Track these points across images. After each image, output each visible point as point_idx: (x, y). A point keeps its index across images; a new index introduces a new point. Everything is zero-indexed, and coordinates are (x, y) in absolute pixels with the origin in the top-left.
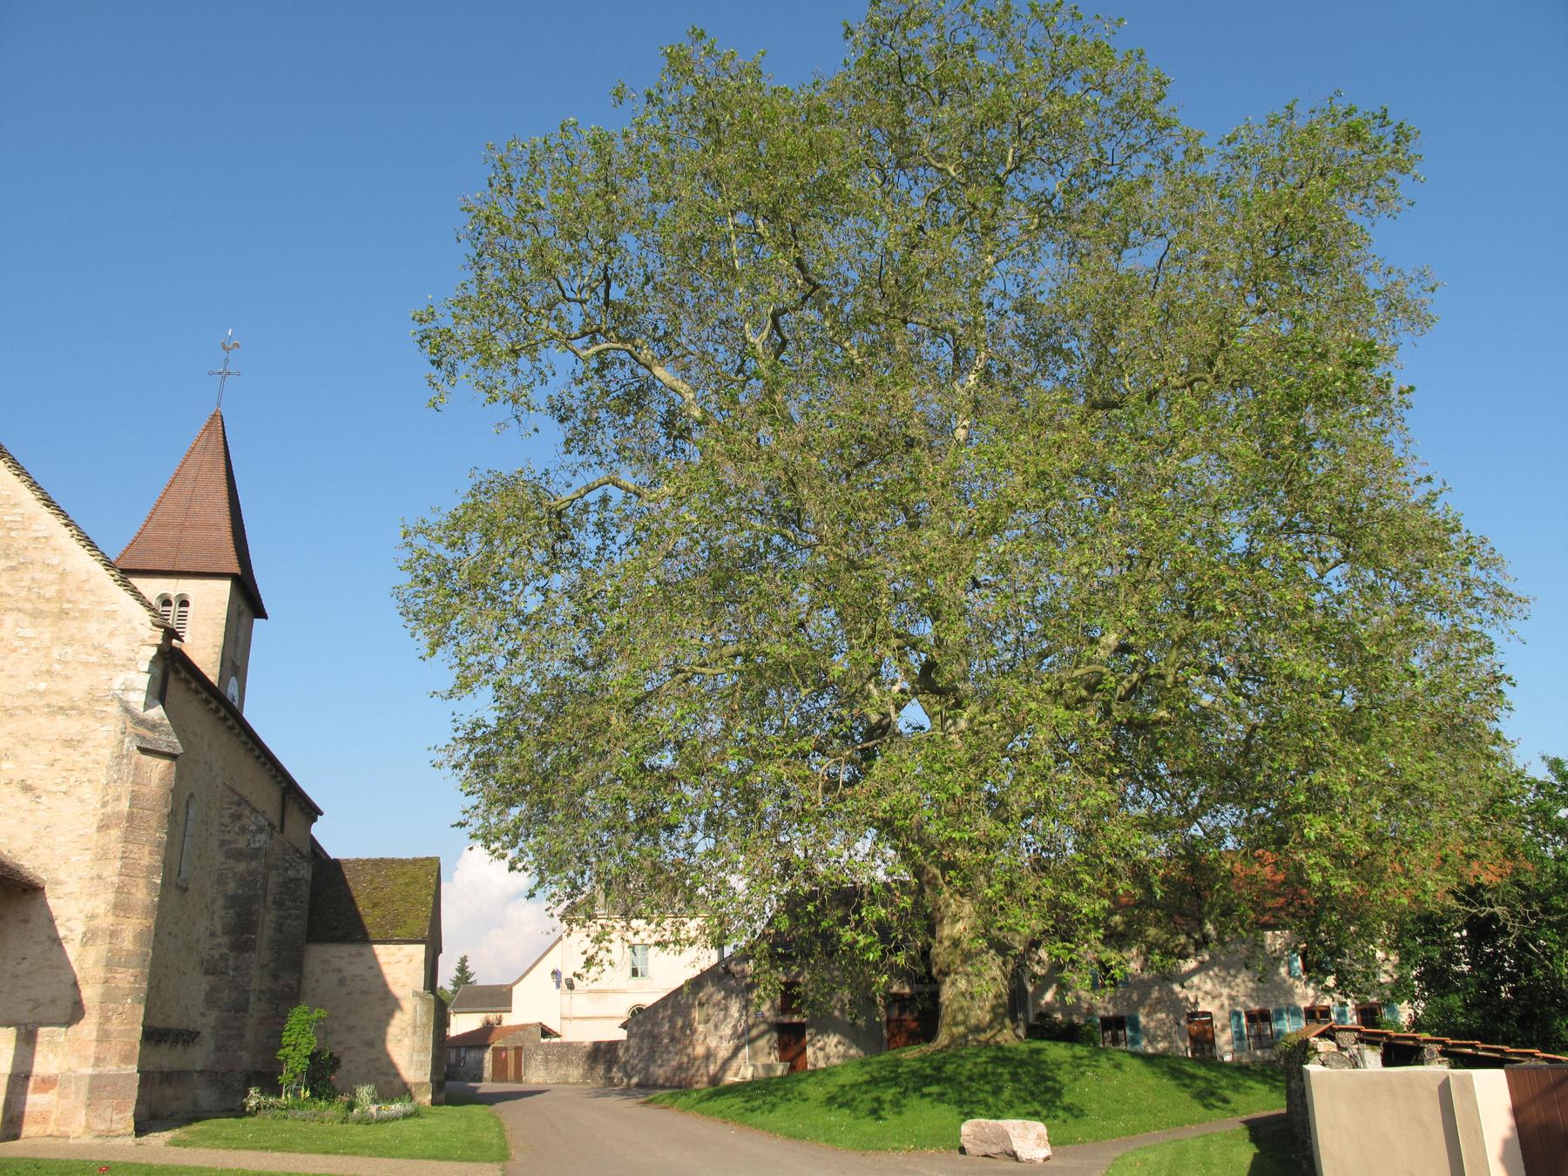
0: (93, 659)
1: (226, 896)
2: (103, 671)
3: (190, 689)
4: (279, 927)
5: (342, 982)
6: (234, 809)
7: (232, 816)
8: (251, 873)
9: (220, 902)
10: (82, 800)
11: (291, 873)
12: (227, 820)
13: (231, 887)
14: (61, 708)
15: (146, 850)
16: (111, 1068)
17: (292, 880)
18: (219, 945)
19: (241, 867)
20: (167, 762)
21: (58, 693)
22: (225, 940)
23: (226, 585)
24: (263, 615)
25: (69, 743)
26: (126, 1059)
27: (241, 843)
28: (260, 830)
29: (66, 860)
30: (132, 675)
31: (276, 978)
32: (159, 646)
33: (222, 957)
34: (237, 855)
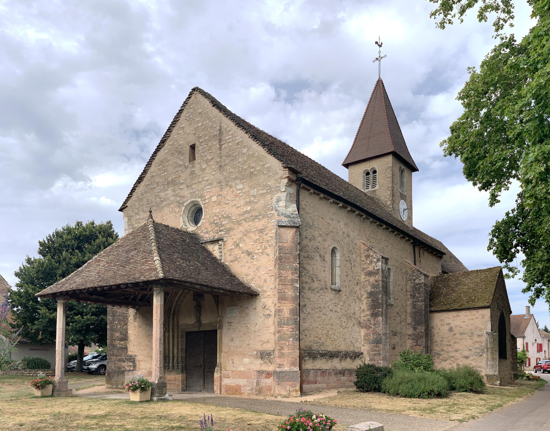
0: (265, 191)
2: (269, 196)
3: (321, 198)
5: (451, 330)
6: (367, 253)
7: (366, 256)
8: (376, 281)
10: (268, 255)
12: (363, 258)
14: (256, 216)
16: (286, 368)
17: (418, 284)
20: (294, 230)
21: (254, 210)
23: (390, 158)
24: (416, 170)
25: (261, 231)
26: (293, 364)
28: (378, 260)
29: (265, 281)
30: (279, 194)
34: (370, 274)
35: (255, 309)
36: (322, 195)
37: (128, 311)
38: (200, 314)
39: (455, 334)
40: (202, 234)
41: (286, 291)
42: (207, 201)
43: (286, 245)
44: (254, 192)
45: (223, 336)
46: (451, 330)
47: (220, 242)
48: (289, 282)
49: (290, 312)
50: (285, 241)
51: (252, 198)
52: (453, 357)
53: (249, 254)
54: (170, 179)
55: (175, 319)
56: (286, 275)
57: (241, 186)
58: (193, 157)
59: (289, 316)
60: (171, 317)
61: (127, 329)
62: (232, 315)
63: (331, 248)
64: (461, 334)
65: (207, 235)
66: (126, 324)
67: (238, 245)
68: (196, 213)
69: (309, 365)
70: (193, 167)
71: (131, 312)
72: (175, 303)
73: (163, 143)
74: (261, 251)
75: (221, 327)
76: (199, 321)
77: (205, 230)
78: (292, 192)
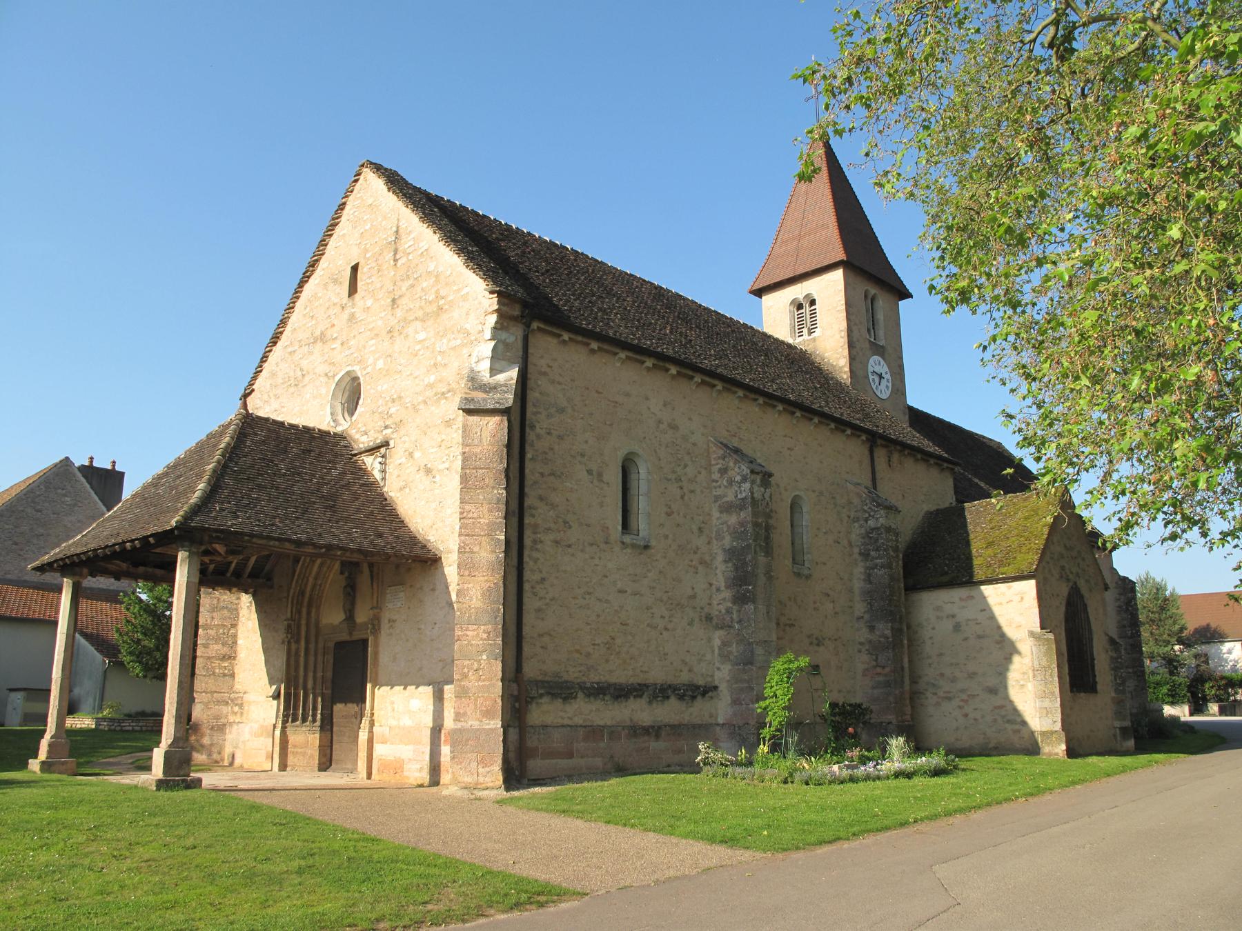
1: (724, 550)
3: (593, 351)
4: (868, 578)
9: (720, 558)
11: (871, 523)
13: (727, 541)
14: (443, 394)
15: (485, 508)
16: (473, 723)
18: (724, 599)
19: (733, 520)
20: (497, 419)
22: (727, 594)
24: (909, 296)
26: (488, 714)
27: (730, 497)
31: (872, 629)
32: (497, 311)
33: (728, 611)
35: (433, 590)
36: (594, 345)
37: (239, 598)
38: (353, 604)
39: (966, 639)
40: (357, 436)
41: (476, 549)
42: (369, 370)
43: (478, 450)
44: (443, 345)
45: (381, 649)
46: (957, 628)
47: (383, 450)
48: (483, 530)
49: (483, 595)
50: (476, 442)
51: (439, 358)
52: (963, 691)
53: (428, 471)
54: (318, 333)
55: (313, 614)
56: (475, 515)
57: (422, 336)
58: (353, 289)
59: (479, 604)
60: (304, 610)
61: (235, 636)
62: (396, 605)
63: (621, 455)
64: (979, 637)
65: (364, 439)
66: (234, 626)
67: (411, 455)
68: (351, 393)
69: (545, 713)
70: (353, 306)
71: (246, 600)
72: (311, 580)
73: (313, 266)
74: (447, 465)
75: (376, 630)
76: (350, 618)
77: (360, 430)
78: (511, 339)
